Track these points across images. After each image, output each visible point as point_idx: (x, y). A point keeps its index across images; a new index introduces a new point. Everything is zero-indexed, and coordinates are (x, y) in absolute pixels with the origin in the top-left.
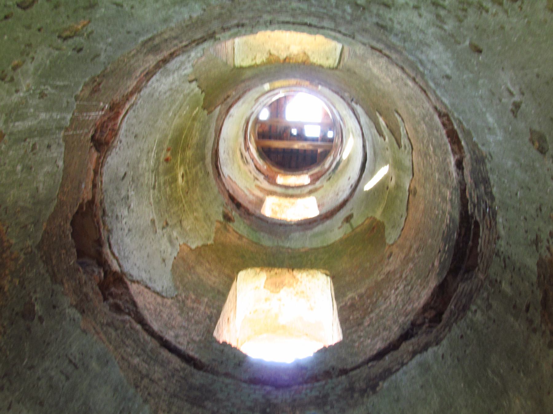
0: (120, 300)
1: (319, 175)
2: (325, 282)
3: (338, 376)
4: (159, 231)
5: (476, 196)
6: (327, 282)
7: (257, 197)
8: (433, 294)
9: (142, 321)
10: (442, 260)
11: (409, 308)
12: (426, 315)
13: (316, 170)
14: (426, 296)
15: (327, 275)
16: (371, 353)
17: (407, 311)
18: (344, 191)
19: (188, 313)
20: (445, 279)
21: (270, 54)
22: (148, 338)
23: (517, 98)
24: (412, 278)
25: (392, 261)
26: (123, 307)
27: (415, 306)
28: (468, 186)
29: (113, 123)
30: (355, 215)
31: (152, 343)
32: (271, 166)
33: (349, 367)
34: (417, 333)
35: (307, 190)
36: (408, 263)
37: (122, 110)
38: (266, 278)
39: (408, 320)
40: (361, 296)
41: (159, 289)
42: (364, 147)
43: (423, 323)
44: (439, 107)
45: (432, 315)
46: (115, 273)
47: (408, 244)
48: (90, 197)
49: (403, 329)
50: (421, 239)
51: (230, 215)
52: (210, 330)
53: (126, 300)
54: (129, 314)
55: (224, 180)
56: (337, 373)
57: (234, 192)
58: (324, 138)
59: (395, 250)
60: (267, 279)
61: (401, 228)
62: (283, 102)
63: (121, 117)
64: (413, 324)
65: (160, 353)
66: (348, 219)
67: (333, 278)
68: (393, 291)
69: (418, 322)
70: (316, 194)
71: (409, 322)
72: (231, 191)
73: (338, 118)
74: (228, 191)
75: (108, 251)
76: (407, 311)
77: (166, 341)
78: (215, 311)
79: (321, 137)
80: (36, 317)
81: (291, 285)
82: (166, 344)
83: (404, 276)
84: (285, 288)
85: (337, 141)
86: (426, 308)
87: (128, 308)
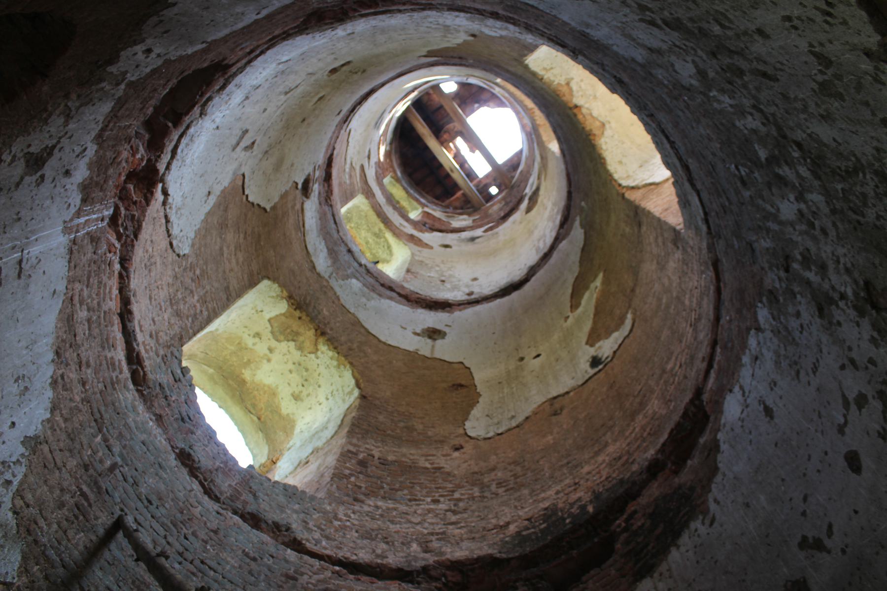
0: (126, 209)
1: (437, 225)
2: (347, 390)
3: (287, 545)
4: (239, 149)
5: (639, 524)
6: (350, 393)
7: (352, 184)
8: (479, 559)
9: (125, 261)
10: (524, 533)
11: (435, 545)
12: (448, 572)
13: (438, 213)
14: (467, 553)
15: (358, 385)
16: (348, 555)
17: (430, 545)
18: (455, 288)
19: (177, 291)
20: (508, 560)
21: (568, 84)
22: (115, 292)
23: (828, 543)
24: (465, 510)
25: (456, 458)
26: (120, 222)
27: (444, 549)
28: (643, 500)
29: (355, 7)
30: (448, 339)
31: (113, 304)
32: (393, 151)
33: (309, 546)
34: (419, 583)
35: (410, 230)
36: (473, 485)
37: (383, 6)
38: (283, 311)
39: (424, 559)
40: (383, 462)
41: (175, 231)
42: (532, 271)
43: (437, 579)
44: (705, 397)
45: (454, 580)
46: (157, 171)
47: (493, 459)
48: (231, 63)
49: (409, 562)
50: (516, 476)
51: (311, 184)
52: (182, 339)
53: (133, 216)
54: (119, 237)
55: (342, 132)
56: (286, 540)
57: (337, 155)
58: (483, 189)
59: (468, 447)
60: (284, 314)
61: (500, 431)
62: (485, 96)
63: (372, 11)
64: (425, 569)
65: (113, 325)
66: (433, 334)
67: (363, 397)
68: (429, 499)
69: (433, 573)
70: (416, 248)
71: (423, 563)
72: (335, 152)
73: (528, 191)
74: (334, 149)
75: (176, 137)
76: (430, 545)
77: (130, 312)
78: (205, 313)
79: (480, 181)
80: (39, 174)
81: (300, 348)
82: (125, 314)
83: (457, 495)
84: (292, 344)
85: (495, 208)
86: (456, 566)
87: (126, 229)
